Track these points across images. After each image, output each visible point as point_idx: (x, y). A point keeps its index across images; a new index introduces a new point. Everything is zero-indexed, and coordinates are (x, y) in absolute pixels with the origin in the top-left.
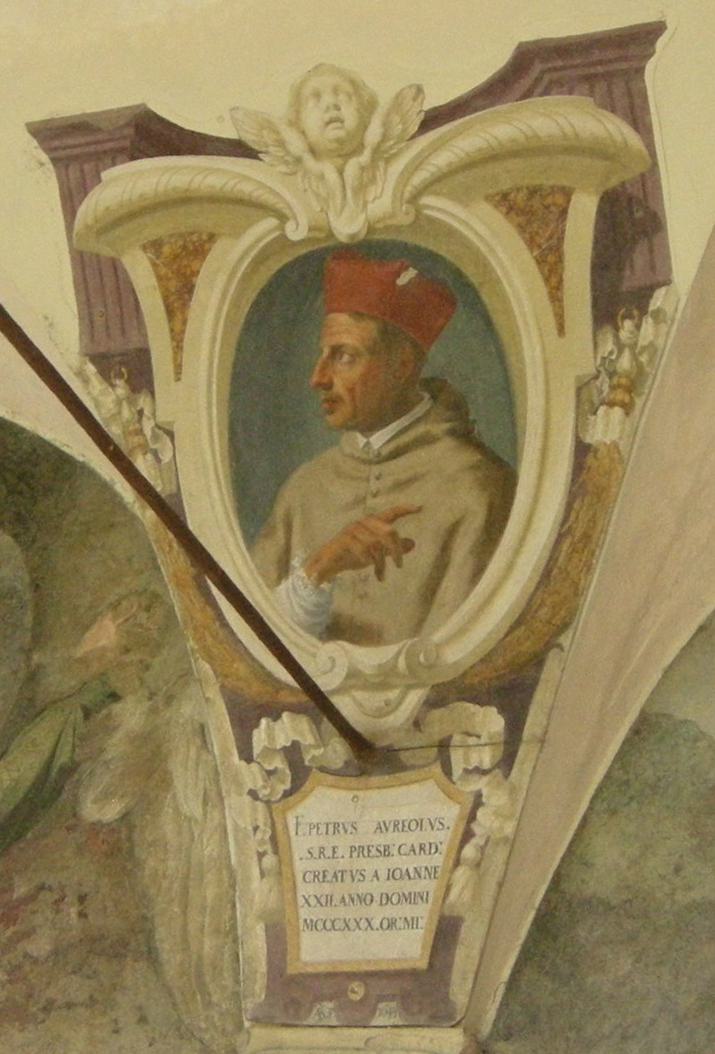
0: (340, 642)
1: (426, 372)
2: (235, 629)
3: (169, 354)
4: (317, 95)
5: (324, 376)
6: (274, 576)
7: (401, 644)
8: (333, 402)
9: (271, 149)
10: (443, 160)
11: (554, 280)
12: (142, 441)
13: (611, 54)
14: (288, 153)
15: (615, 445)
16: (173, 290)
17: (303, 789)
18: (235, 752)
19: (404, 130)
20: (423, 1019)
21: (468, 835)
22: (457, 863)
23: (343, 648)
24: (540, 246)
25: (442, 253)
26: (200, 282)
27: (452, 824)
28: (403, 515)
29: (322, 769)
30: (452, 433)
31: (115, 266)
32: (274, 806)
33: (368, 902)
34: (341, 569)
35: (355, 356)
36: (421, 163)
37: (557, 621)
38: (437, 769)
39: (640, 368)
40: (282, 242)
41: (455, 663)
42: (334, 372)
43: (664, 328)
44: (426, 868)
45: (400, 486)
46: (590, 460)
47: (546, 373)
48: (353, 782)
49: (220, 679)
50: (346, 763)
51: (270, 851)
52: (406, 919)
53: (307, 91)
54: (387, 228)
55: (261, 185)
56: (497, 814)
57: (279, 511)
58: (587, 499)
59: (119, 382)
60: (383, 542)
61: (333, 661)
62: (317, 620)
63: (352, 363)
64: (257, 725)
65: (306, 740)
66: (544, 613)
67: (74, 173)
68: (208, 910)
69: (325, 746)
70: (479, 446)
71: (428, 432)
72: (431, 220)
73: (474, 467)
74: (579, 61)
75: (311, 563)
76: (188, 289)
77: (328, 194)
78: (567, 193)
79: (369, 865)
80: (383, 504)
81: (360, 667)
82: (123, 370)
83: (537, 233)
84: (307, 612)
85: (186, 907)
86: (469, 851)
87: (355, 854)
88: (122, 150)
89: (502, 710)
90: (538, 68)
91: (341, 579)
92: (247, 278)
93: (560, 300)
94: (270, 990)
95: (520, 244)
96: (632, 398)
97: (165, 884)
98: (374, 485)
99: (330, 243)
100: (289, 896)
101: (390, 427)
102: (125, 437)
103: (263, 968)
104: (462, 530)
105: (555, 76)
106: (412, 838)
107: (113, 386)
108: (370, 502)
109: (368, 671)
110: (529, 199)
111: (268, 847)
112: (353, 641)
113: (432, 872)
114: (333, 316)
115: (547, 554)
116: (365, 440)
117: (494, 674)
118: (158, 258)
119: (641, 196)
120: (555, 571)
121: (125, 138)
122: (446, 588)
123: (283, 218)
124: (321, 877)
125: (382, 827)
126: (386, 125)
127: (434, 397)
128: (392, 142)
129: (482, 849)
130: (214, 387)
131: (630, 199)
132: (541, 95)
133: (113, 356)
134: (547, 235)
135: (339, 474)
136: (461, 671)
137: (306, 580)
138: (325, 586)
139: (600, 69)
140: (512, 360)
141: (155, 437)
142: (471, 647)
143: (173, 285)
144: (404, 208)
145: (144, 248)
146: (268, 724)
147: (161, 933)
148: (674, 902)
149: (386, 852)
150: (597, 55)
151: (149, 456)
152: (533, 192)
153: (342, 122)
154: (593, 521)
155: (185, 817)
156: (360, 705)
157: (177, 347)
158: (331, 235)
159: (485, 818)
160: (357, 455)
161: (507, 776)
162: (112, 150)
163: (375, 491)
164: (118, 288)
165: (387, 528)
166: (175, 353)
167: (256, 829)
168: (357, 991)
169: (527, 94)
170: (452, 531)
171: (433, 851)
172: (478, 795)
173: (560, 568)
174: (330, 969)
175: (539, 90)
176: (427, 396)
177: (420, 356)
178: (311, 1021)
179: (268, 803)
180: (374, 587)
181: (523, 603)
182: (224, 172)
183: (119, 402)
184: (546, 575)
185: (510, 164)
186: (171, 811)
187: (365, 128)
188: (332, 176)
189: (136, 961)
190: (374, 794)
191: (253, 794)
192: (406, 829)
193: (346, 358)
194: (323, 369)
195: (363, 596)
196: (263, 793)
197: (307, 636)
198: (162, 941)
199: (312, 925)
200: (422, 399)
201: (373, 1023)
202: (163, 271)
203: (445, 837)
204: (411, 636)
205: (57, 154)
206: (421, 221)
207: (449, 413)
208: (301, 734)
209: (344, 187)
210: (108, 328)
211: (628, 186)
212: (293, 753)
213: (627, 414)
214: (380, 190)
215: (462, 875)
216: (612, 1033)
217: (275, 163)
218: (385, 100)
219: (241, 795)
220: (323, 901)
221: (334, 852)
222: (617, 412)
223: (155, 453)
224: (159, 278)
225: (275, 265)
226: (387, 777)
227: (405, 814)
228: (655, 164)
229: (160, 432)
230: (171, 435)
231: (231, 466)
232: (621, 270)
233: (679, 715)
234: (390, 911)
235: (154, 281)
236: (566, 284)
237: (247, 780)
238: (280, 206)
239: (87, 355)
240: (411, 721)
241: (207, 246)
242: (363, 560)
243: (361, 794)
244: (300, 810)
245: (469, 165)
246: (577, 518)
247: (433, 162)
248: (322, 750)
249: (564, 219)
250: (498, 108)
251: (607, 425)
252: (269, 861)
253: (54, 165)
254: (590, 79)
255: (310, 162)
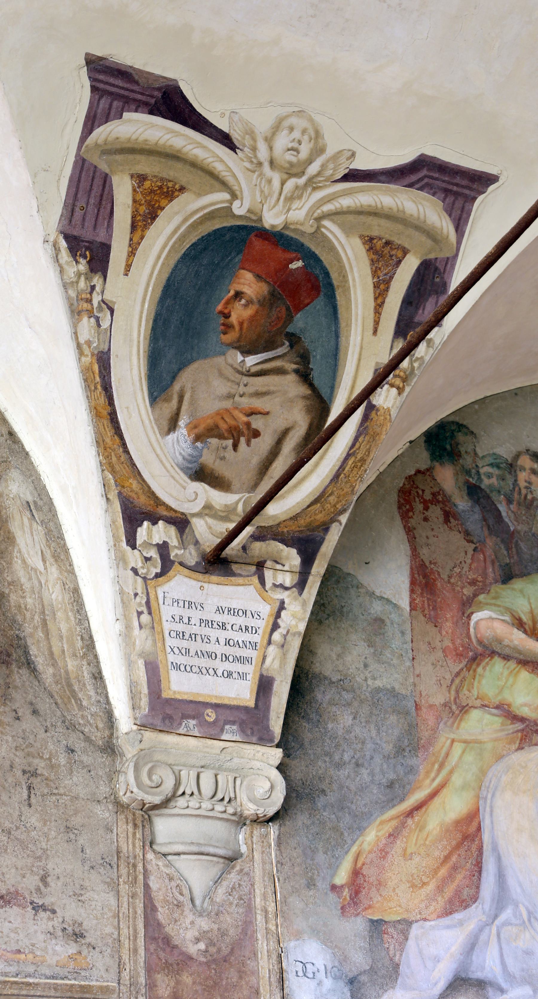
0: (203, 484)
1: (290, 329)
2: (133, 457)
3: (125, 255)
4: (291, 129)
5: (226, 308)
6: (166, 429)
7: (241, 495)
8: (228, 327)
9: (246, 149)
10: (346, 202)
11: (379, 301)
12: (89, 307)
13: (465, 182)
14: (256, 157)
15: (389, 410)
16: (141, 213)
17: (168, 575)
18: (124, 538)
19: (332, 175)
20: (254, 739)
21: (275, 626)
22: (269, 643)
23: (204, 488)
24: (379, 278)
25: (322, 258)
26: (162, 215)
27: (266, 617)
28: (256, 414)
29: (181, 564)
30: (297, 371)
31: (106, 179)
32: (149, 582)
33: (214, 658)
34: (212, 436)
35: (250, 302)
36: (333, 199)
37: (339, 506)
38: (255, 580)
39: (413, 368)
40: (228, 211)
41: (273, 516)
42: (233, 308)
43: (431, 351)
44: (250, 642)
45: (258, 394)
46: (373, 414)
47: (360, 355)
48: (200, 576)
49: (118, 488)
50: (197, 562)
51: (145, 611)
52: (239, 673)
53: (286, 123)
54: (295, 230)
55: (230, 170)
56: (294, 616)
57: (177, 387)
58: (367, 438)
59: (83, 261)
60: (241, 427)
61: (197, 494)
62: (190, 466)
63: (246, 306)
64: (141, 525)
65: (172, 542)
66: (332, 499)
67: (104, 103)
68: (65, 639)
69: (185, 549)
70: (311, 385)
71: (283, 366)
72: (323, 235)
73: (305, 397)
74: (446, 179)
75: (192, 427)
76: (153, 216)
77: (269, 194)
78: (405, 252)
79: (214, 633)
80: (246, 402)
81: (214, 503)
82: (87, 253)
83: (380, 269)
84: (184, 458)
85: (48, 634)
86: (276, 636)
87: (203, 625)
88: (146, 104)
89: (300, 552)
90: (424, 172)
91: (210, 443)
92: (194, 226)
93: (380, 314)
94: (152, 708)
95: (367, 270)
96: (404, 386)
97: (28, 615)
98: (242, 389)
99: (259, 225)
100: (159, 645)
101: (259, 355)
102: (77, 300)
103: (145, 690)
104: (291, 434)
105: (431, 181)
106: (241, 621)
107: (77, 262)
108: (237, 398)
109: (218, 507)
110: (383, 247)
111: (144, 609)
112: (209, 484)
113: (254, 646)
114: (242, 271)
115: (339, 464)
116: (242, 358)
117: (298, 529)
118: (139, 187)
119: (442, 270)
120: (342, 475)
121: (152, 96)
122: (276, 467)
123: (234, 196)
124: (181, 635)
125: (220, 610)
126: (323, 166)
127: (291, 346)
128: (322, 179)
129: (285, 636)
130: (151, 289)
131: (436, 269)
132: (418, 189)
133: (83, 241)
134: (385, 272)
135: (221, 374)
136: (277, 522)
137: (186, 438)
138: (199, 444)
139: (455, 188)
140: (342, 339)
141: (100, 309)
142: (285, 509)
143: (143, 209)
144: (311, 222)
145: (132, 176)
146: (148, 526)
147: (33, 650)
148: (368, 686)
149: (223, 626)
150: (458, 180)
151: (93, 320)
152: (388, 243)
153: (298, 152)
154: (369, 451)
155: (32, 568)
156: (210, 528)
157: (132, 252)
158: (260, 219)
159: (286, 618)
160: (235, 366)
161: (300, 594)
162: (140, 100)
163: (241, 393)
164: (102, 196)
165: (245, 419)
166: (129, 256)
167: (136, 595)
168: (211, 716)
169: (410, 185)
170: (285, 432)
171: (254, 632)
172: (282, 602)
173: (345, 474)
174: (191, 698)
175: (417, 186)
176: (287, 343)
177: (290, 318)
178: (181, 731)
179: (145, 579)
180: (230, 454)
181: (321, 490)
182: (210, 150)
183: (79, 275)
184: (337, 476)
185: (383, 222)
186: (20, 562)
187: (310, 163)
188: (276, 183)
189: (19, 668)
190: (214, 587)
191: (135, 571)
192: (236, 614)
193: (243, 301)
194: (228, 303)
195: (223, 458)
196: (141, 571)
197: (182, 475)
198: (36, 657)
199: (177, 667)
200: (283, 344)
201: (223, 737)
202: (139, 197)
203: (263, 625)
204: (249, 492)
205: (94, 84)
206: (317, 233)
207: (298, 359)
208: (170, 538)
209: (280, 194)
210: (84, 219)
211: (438, 261)
212: (163, 548)
213: (399, 394)
214: (301, 204)
215: (272, 650)
216: (350, 761)
217: (245, 159)
218: (330, 152)
219: (125, 569)
220: (183, 651)
221: (189, 621)
222: (394, 391)
223: (97, 319)
224: (134, 201)
225: (217, 225)
226: (222, 578)
227: (235, 605)
228: (457, 255)
229: (104, 306)
230: (112, 311)
231: (150, 345)
232: (417, 308)
233: (345, 570)
234: (228, 666)
235: (130, 202)
236: (386, 305)
237: (131, 560)
238: (236, 188)
239: (61, 232)
240: (241, 545)
241: (177, 193)
242: (226, 435)
243: (206, 585)
244: (166, 587)
245: (360, 212)
246: (360, 447)
247: (340, 201)
248: (182, 551)
249: (397, 267)
250: (392, 186)
251: (387, 397)
252: (145, 618)
253: (92, 91)
254: (447, 191)
255: (266, 167)
